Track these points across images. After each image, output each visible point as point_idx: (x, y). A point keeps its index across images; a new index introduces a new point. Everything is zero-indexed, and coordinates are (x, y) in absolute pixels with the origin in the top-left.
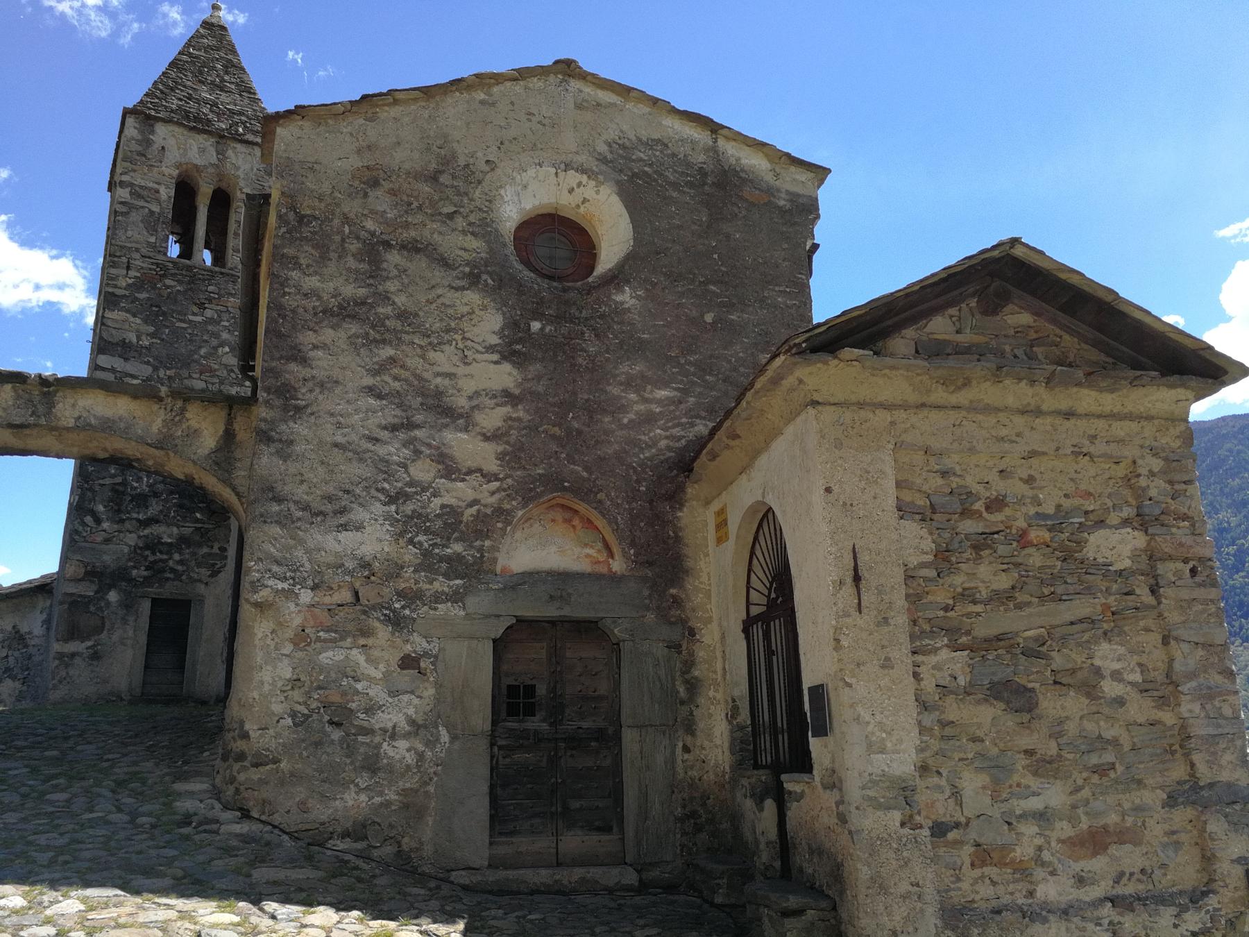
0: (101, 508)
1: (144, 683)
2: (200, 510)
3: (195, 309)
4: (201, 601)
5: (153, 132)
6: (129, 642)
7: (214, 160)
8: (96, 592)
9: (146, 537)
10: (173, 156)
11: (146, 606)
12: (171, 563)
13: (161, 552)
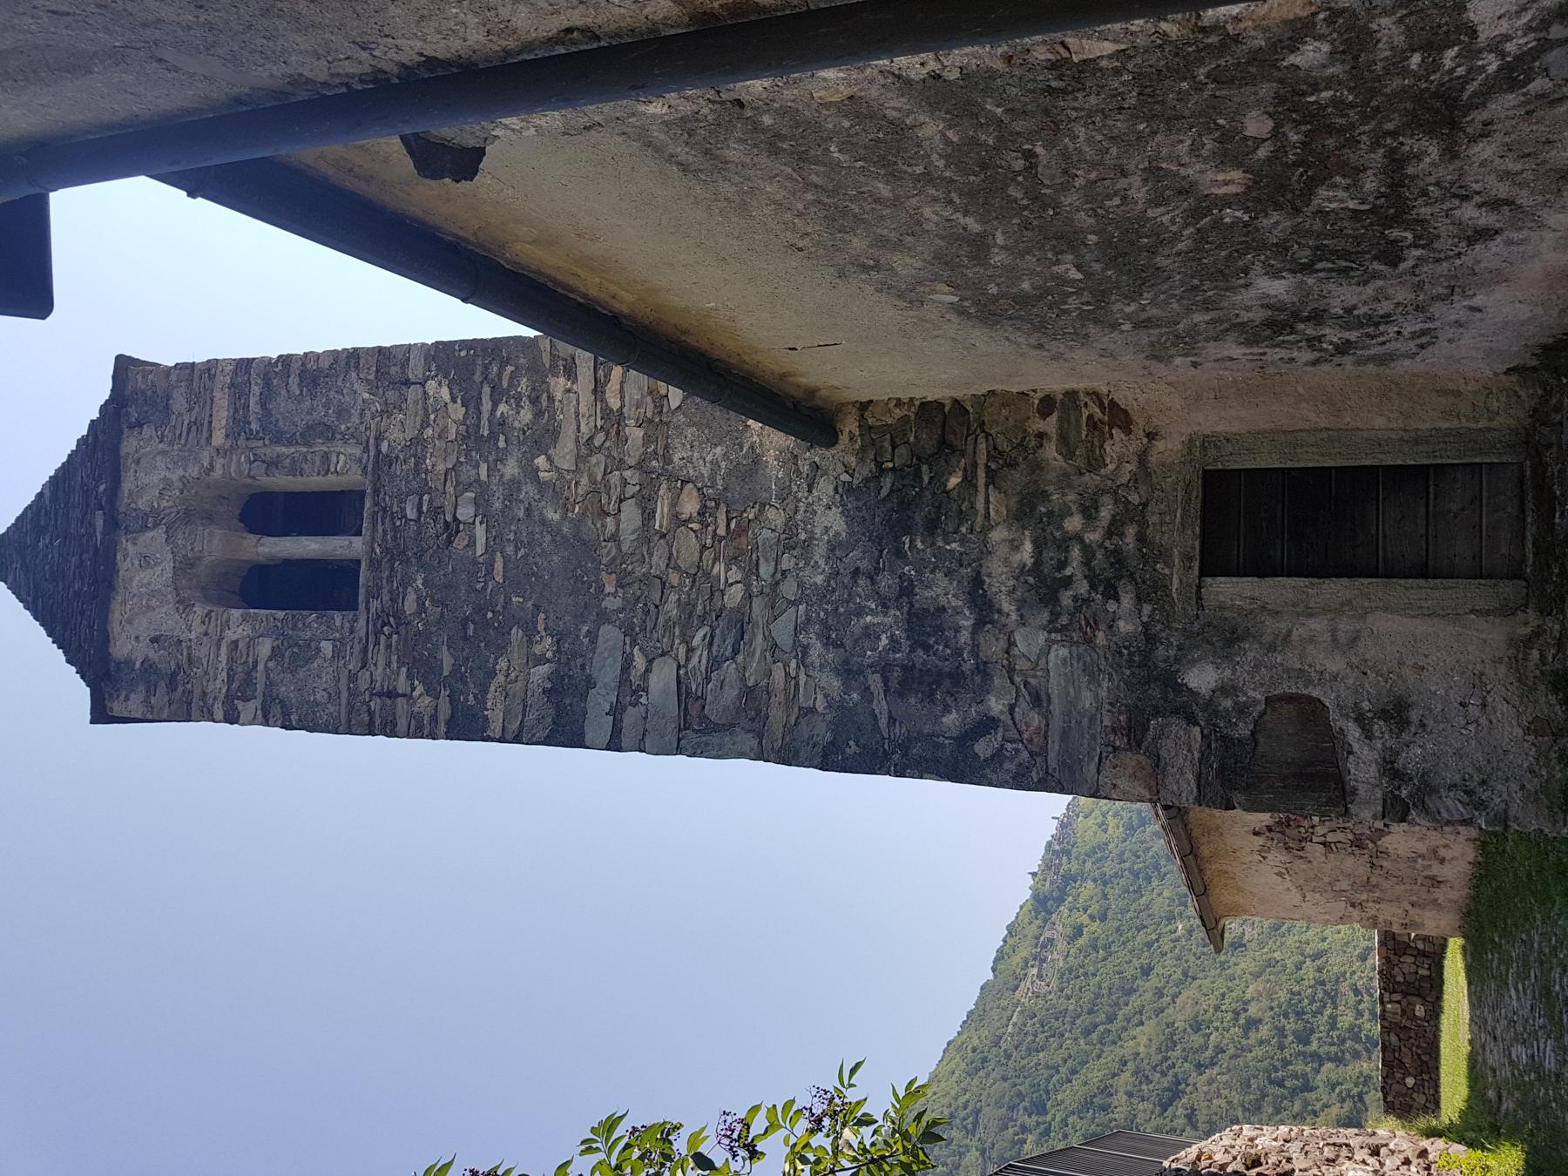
0: (951, 720)
1: (1477, 573)
2: (938, 479)
3: (460, 542)
4: (1208, 442)
5: (129, 662)
6: (1345, 626)
7: (159, 534)
8: (1192, 720)
9: (1021, 604)
10: (166, 619)
11: (1227, 590)
12: (1093, 537)
13: (1062, 565)
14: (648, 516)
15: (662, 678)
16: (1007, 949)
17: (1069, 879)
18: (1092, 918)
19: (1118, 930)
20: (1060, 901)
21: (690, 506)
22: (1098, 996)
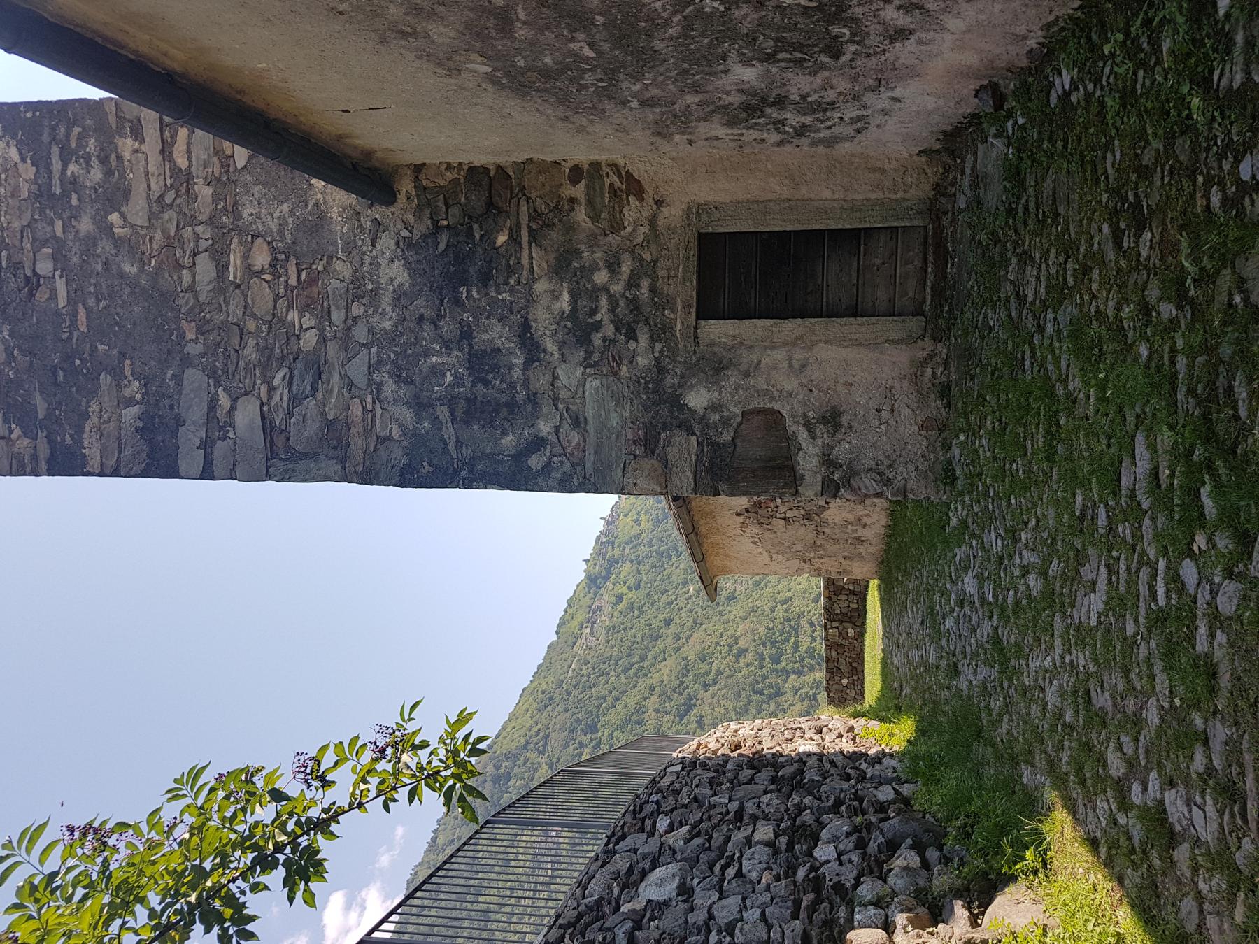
0: (508, 441)
2: (488, 236)
3: (42, 296)
6: (798, 355)
8: (691, 432)
9: (562, 345)
11: (717, 330)
12: (617, 288)
13: (593, 312)
14: (222, 268)
15: (247, 415)
16: (567, 617)
17: (613, 562)
18: (630, 588)
19: (648, 595)
20: (607, 578)
21: (261, 258)
22: (634, 643)
